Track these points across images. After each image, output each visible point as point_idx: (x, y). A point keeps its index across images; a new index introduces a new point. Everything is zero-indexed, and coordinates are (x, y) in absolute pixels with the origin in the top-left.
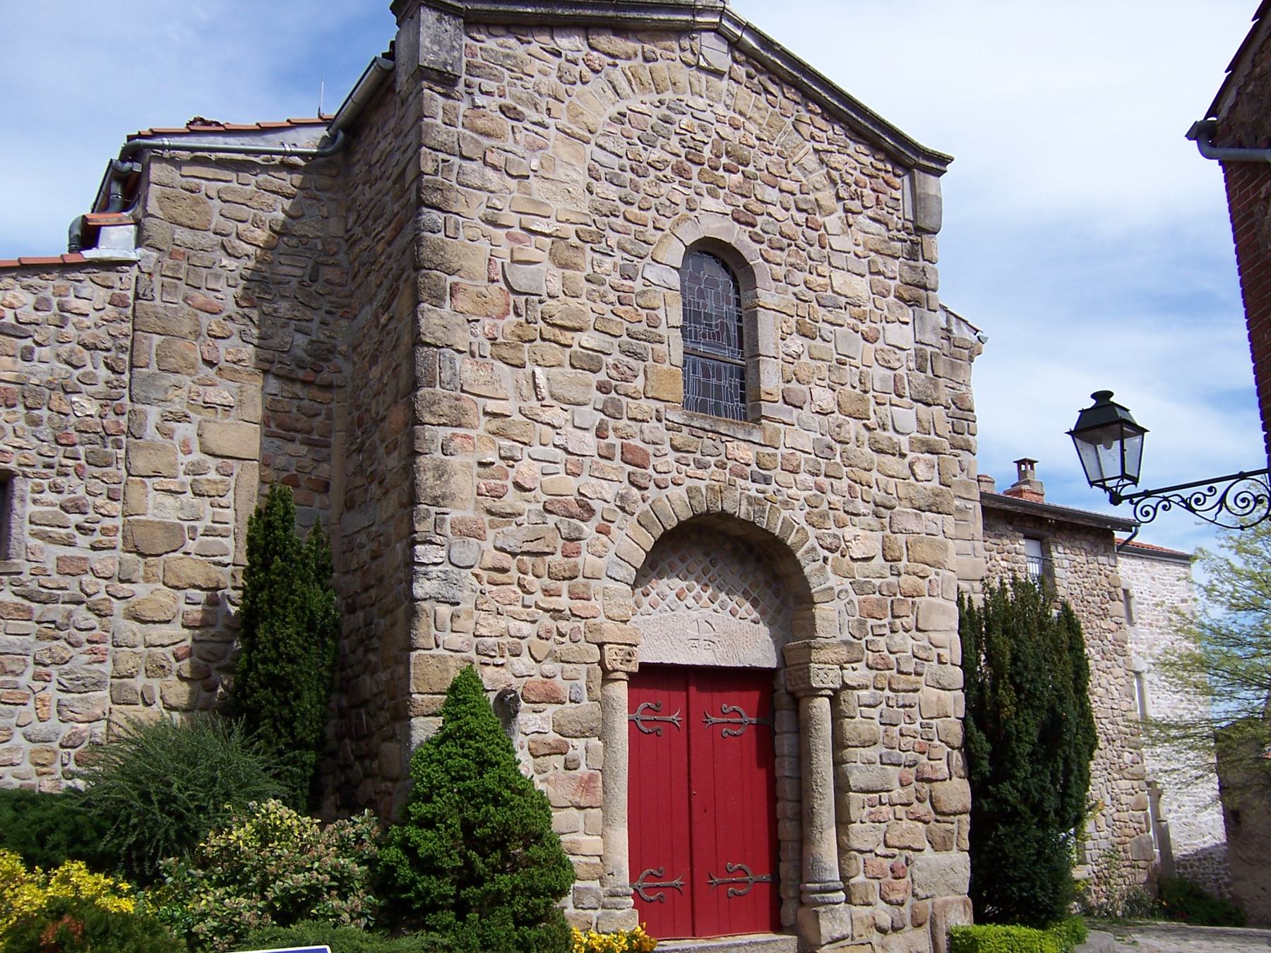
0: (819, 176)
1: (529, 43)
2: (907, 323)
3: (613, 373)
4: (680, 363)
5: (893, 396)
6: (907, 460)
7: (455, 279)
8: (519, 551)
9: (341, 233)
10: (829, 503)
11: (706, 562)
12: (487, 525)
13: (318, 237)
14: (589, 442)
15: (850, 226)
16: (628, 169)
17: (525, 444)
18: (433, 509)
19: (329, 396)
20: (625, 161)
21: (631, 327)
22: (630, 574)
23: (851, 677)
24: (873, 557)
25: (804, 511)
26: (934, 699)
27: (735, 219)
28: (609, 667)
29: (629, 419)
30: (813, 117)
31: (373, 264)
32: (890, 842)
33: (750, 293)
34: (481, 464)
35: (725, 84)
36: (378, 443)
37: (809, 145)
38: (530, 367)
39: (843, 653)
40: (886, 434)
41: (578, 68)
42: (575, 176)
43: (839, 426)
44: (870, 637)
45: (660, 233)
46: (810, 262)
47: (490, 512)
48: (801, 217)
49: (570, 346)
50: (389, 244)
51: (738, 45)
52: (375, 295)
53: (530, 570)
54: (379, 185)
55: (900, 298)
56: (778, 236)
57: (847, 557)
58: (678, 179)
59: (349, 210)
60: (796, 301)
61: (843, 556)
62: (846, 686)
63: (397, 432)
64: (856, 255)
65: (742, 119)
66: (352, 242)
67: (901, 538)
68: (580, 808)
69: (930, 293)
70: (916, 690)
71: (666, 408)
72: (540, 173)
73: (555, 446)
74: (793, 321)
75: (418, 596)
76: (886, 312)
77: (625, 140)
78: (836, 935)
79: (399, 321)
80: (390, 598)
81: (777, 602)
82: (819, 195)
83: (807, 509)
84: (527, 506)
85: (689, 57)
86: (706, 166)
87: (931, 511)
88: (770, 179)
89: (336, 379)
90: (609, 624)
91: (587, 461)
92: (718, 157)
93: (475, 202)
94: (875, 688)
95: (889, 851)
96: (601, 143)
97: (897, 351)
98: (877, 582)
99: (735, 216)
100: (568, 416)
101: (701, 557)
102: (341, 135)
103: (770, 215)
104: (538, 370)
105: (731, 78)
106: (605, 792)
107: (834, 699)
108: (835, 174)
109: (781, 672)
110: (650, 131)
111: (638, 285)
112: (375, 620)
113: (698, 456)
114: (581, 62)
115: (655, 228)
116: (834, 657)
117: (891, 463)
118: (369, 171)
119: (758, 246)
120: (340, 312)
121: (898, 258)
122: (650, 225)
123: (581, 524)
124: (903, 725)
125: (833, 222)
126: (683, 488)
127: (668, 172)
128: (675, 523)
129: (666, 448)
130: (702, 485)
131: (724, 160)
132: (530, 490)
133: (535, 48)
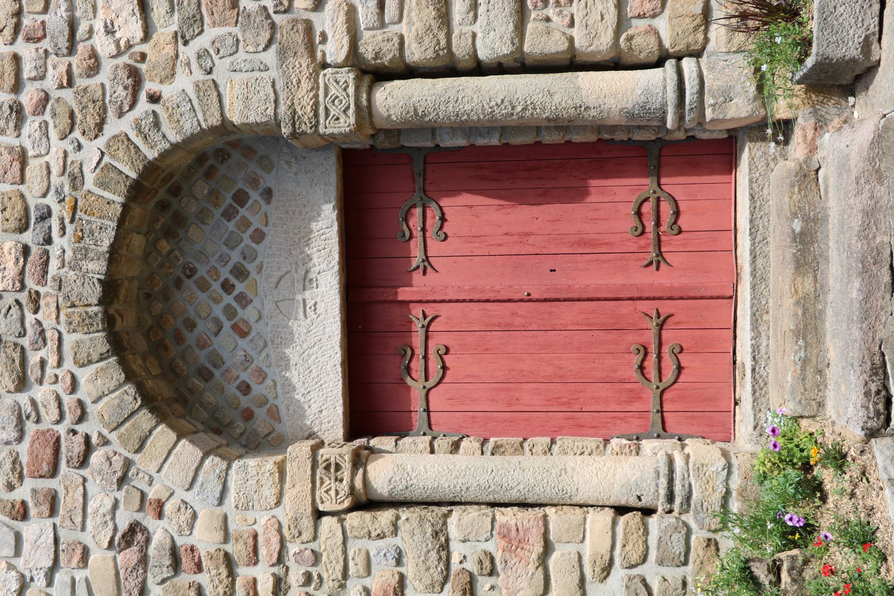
10: (61, 87)
25: (82, 140)
57: (145, 48)
62: (354, 59)
68: (547, 548)
81: (236, 155)
83: (77, 134)
116: (305, 85)
126: (78, 372)
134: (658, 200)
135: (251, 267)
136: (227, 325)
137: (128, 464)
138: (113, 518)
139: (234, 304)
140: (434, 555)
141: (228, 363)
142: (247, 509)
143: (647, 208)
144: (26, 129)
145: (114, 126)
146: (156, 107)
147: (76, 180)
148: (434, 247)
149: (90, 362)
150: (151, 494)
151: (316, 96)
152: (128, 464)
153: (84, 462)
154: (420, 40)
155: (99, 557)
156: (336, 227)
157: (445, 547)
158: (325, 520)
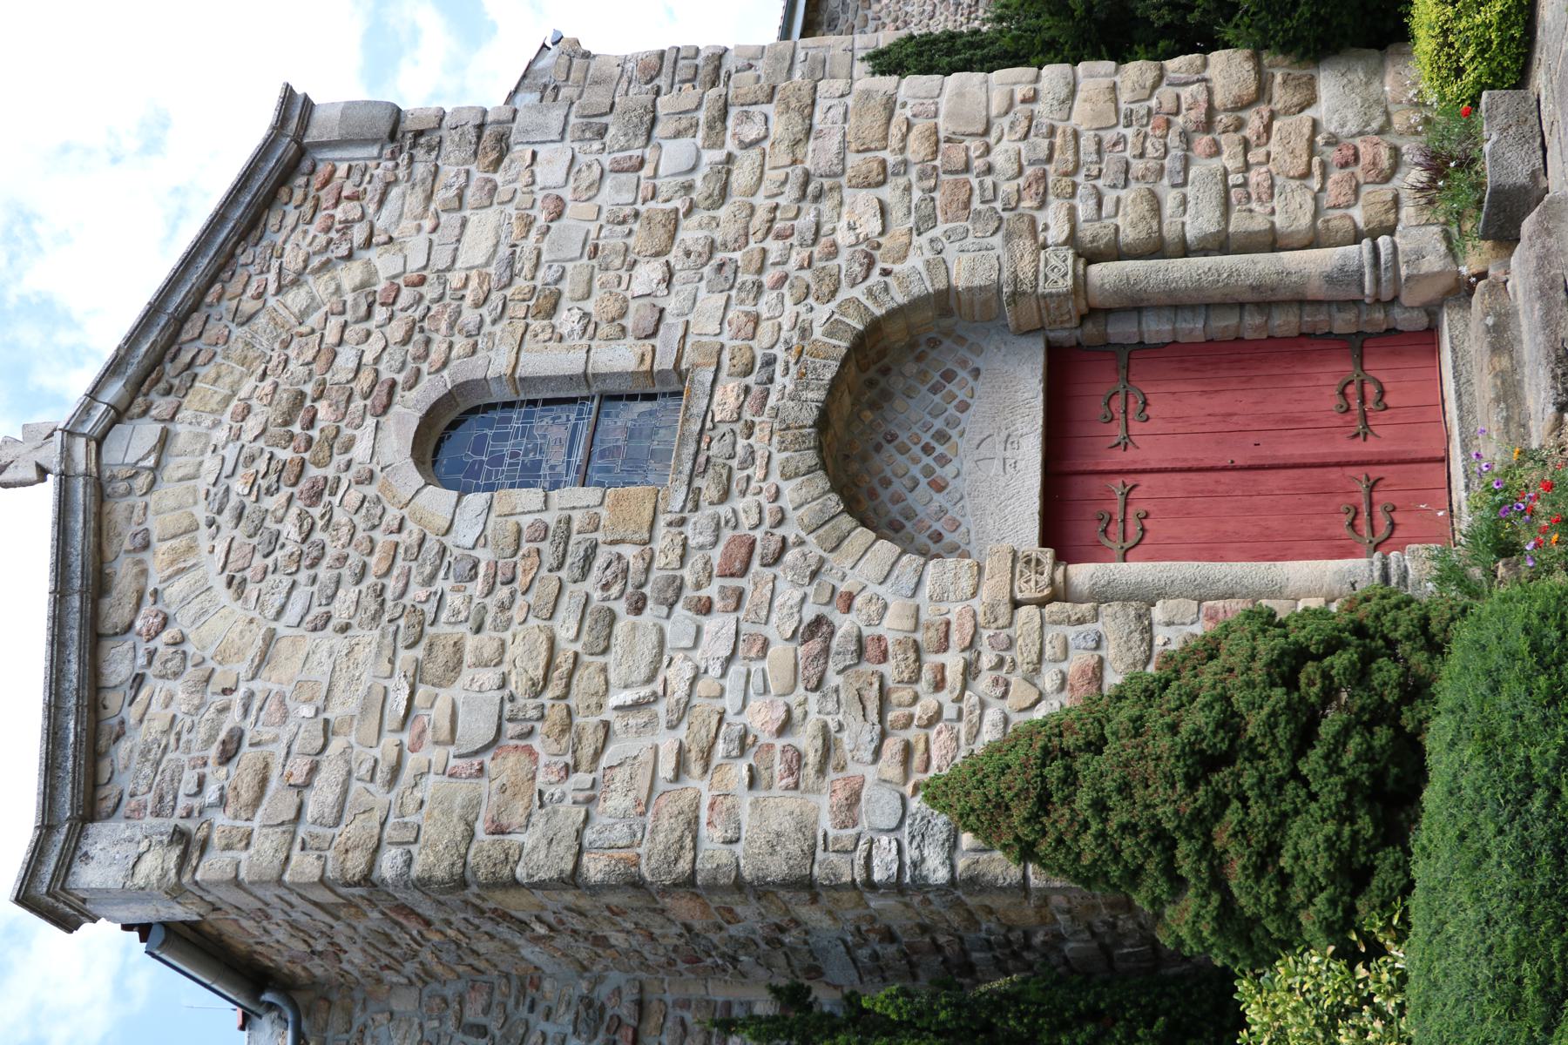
0: (320, 287)
1: (122, 722)
2: (534, 154)
3: (615, 590)
4: (599, 492)
5: (642, 173)
6: (737, 152)
7: (480, 827)
8: (878, 728)
9: (414, 993)
10: (801, 268)
11: (890, 449)
12: (840, 775)
13: (421, 1026)
14: (719, 626)
15: (391, 239)
16: (312, 572)
17: (720, 721)
18: (820, 855)
19: (655, 1005)
20: (303, 576)
21: (546, 566)
22: (910, 561)
23: (1057, 231)
24: (880, 201)
25: (814, 304)
26: (1088, 106)
27: (386, 407)
28: (1046, 592)
29: (682, 565)
30: (227, 295)
31: (459, 946)
32: (1302, 168)
33: (494, 387)
34: (752, 784)
35: (182, 429)
36: (724, 934)
37: (272, 302)
38: (608, 715)
39: (1026, 244)
40: (699, 183)
41: (161, 649)
42: (325, 647)
43: (688, 254)
44: (998, 205)
45: (409, 524)
46: (447, 300)
47: (821, 771)
48: (380, 313)
49: (576, 655)
50: (428, 923)
51: (121, 408)
52: (505, 942)
53: (907, 711)
54: (341, 940)
55: (498, 162)
56: (410, 347)
57: (881, 240)
58: (326, 498)
59: (379, 981)
60: (505, 321)
61: (879, 246)
62: (1072, 240)
63: (706, 905)
64: (434, 230)
65: (235, 402)
66: (427, 975)
67: (853, 159)
69: (490, 118)
70: (1076, 135)
71: (666, 512)
72: (320, 703)
73: (723, 675)
74: (536, 325)
75: (947, 876)
76: (518, 185)
77: (269, 577)
78: (1442, 248)
79: (543, 908)
80: (951, 916)
81: (947, 343)
82: (347, 285)
83: (811, 301)
84: (813, 716)
85: (142, 481)
86: (307, 456)
87: (811, 115)
88: (323, 359)
89: (630, 994)
90: (985, 593)
91: (745, 627)
92: (292, 437)
93: (366, 798)
94: (1073, 195)
95: (1316, 170)
96: (274, 611)
97: (575, 169)
98: (917, 195)
99: (379, 410)
100: (679, 656)
101: (884, 455)
102: (268, 997)
103: (377, 360)
104: (614, 700)
105: (172, 418)
106: (1232, 596)
107: (1090, 256)
108: (316, 262)
109: (1051, 335)
110: (255, 541)
111: (484, 555)
112: (983, 935)
113: (735, 463)
114: (151, 645)
115: (400, 529)
116: (1028, 258)
117: (741, 177)
118: (320, 954)
119: (425, 379)
120: (531, 991)
121: (437, 167)
122: (395, 537)
123: (839, 633)
124: (1128, 154)
125: (385, 264)
127: (316, 512)
128: (834, 497)
129: (724, 511)
130: (778, 458)
131: (296, 428)
132: (789, 711)
133: (132, 714)
134: (1362, 383)
135: (954, 433)
136: (923, 482)
137: (822, 561)
138: (800, 611)
139: (933, 464)
140: (1137, 636)
141: (921, 515)
142: (941, 601)
143: (1350, 390)
144: (764, 299)
145: (845, 293)
146: (887, 279)
147: (805, 332)
148: (1136, 427)
149: (797, 475)
150: (843, 588)
151: (1037, 266)
152: (822, 561)
153: (777, 559)
154: (1134, 225)
155: (778, 649)
156: (1041, 397)
157: (1148, 630)
158: (1023, 610)
